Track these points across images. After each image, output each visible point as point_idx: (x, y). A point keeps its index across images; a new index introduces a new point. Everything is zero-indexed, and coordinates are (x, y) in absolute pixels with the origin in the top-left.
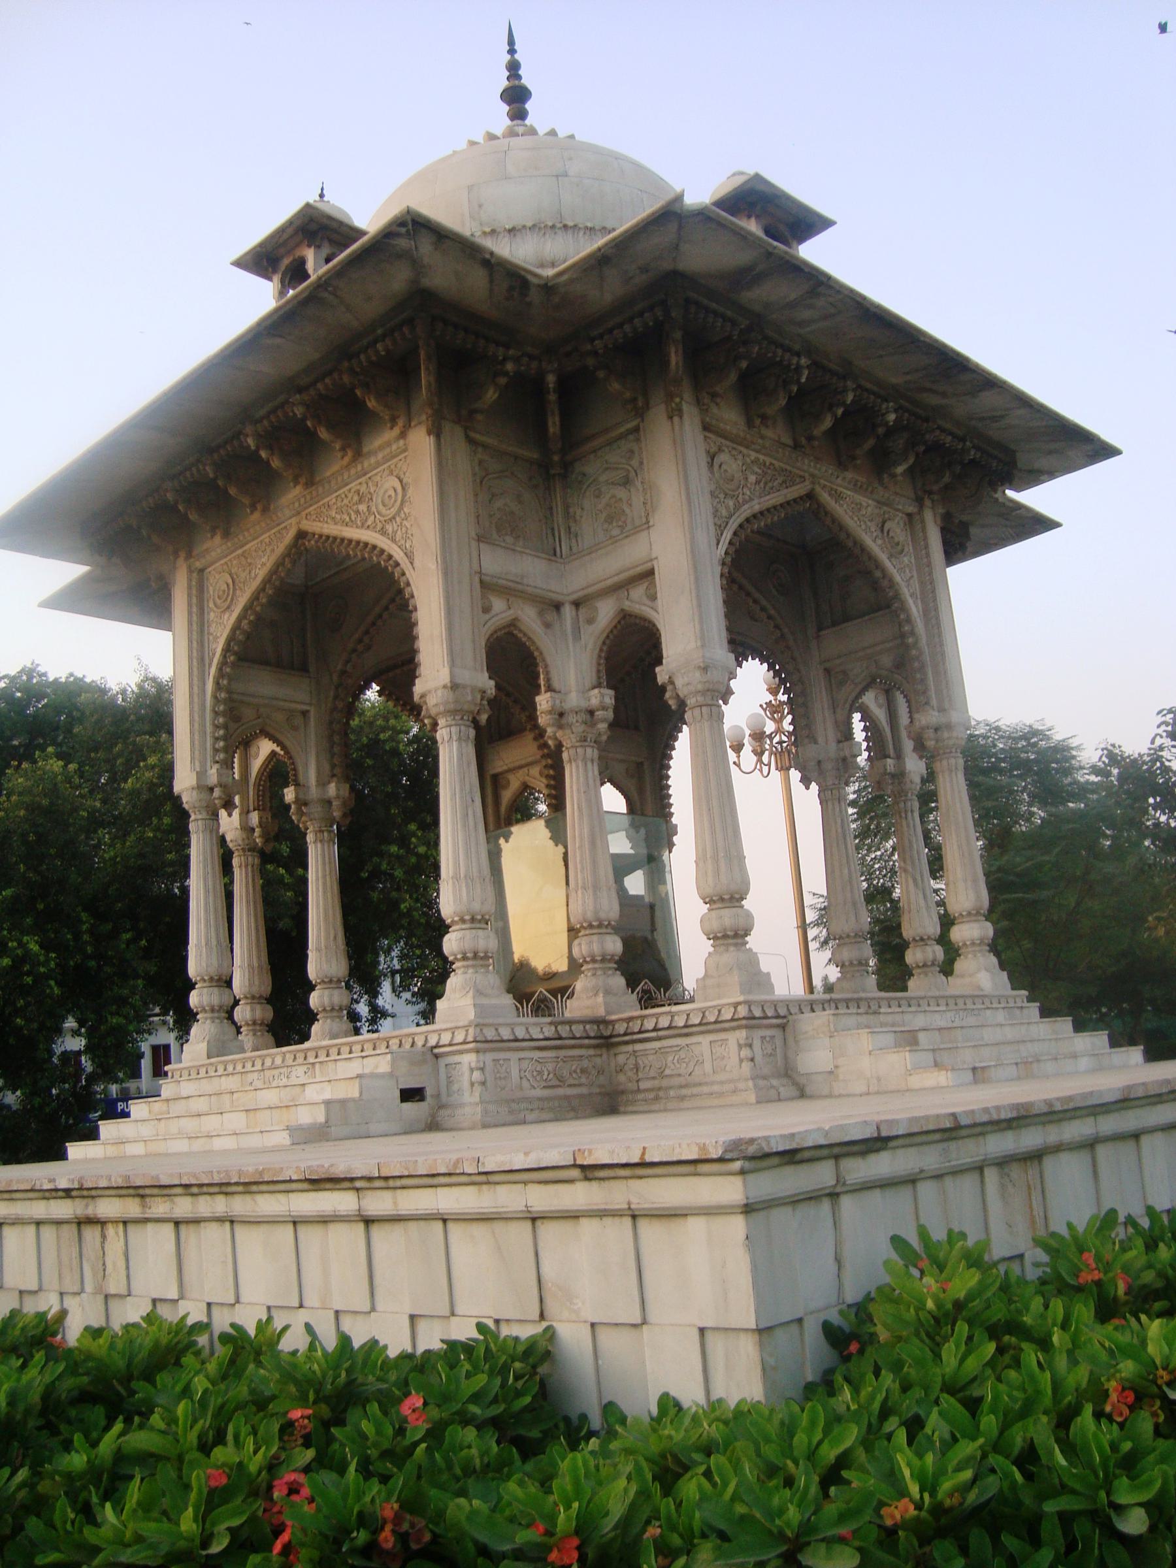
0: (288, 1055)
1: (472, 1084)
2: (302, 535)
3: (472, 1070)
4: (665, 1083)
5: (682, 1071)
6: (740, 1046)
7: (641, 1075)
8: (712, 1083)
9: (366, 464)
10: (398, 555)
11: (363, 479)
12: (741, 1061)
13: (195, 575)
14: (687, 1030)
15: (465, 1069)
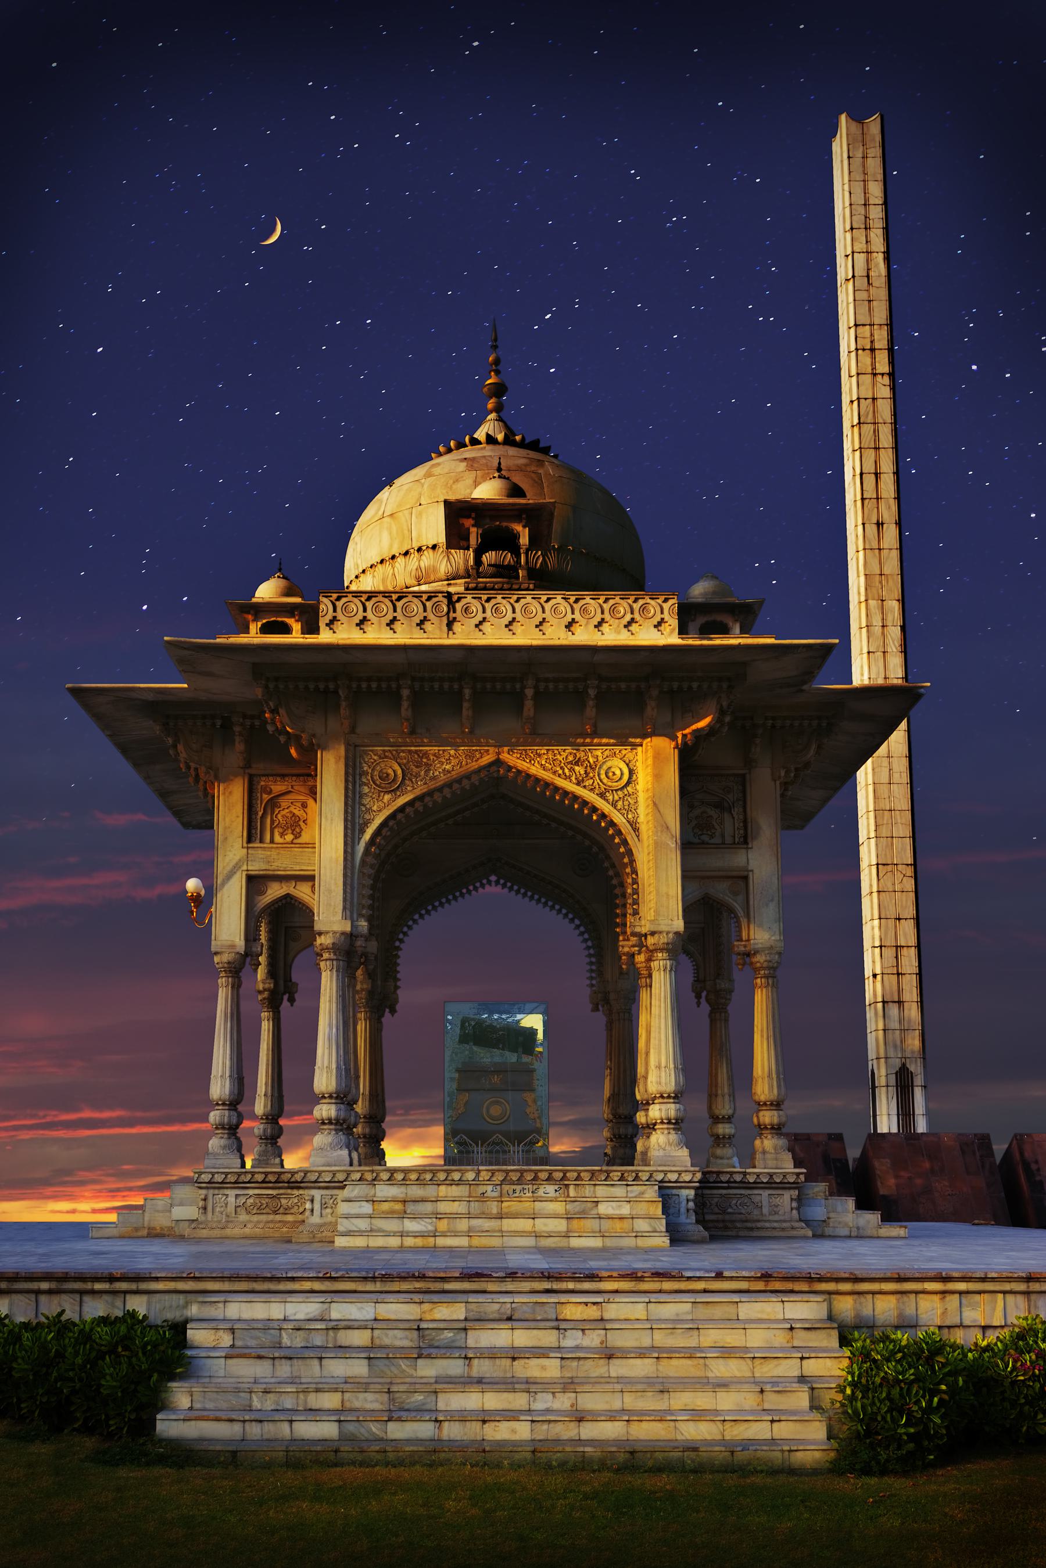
0: (483, 1174)
1: (688, 1210)
2: (498, 762)
3: (688, 1200)
4: (727, 1217)
5: (743, 1211)
6: (792, 1199)
7: (705, 1210)
8: (769, 1221)
9: (595, 741)
10: (618, 818)
11: (582, 748)
12: (792, 1209)
13: (352, 748)
14: (757, 1185)
15: (683, 1198)
